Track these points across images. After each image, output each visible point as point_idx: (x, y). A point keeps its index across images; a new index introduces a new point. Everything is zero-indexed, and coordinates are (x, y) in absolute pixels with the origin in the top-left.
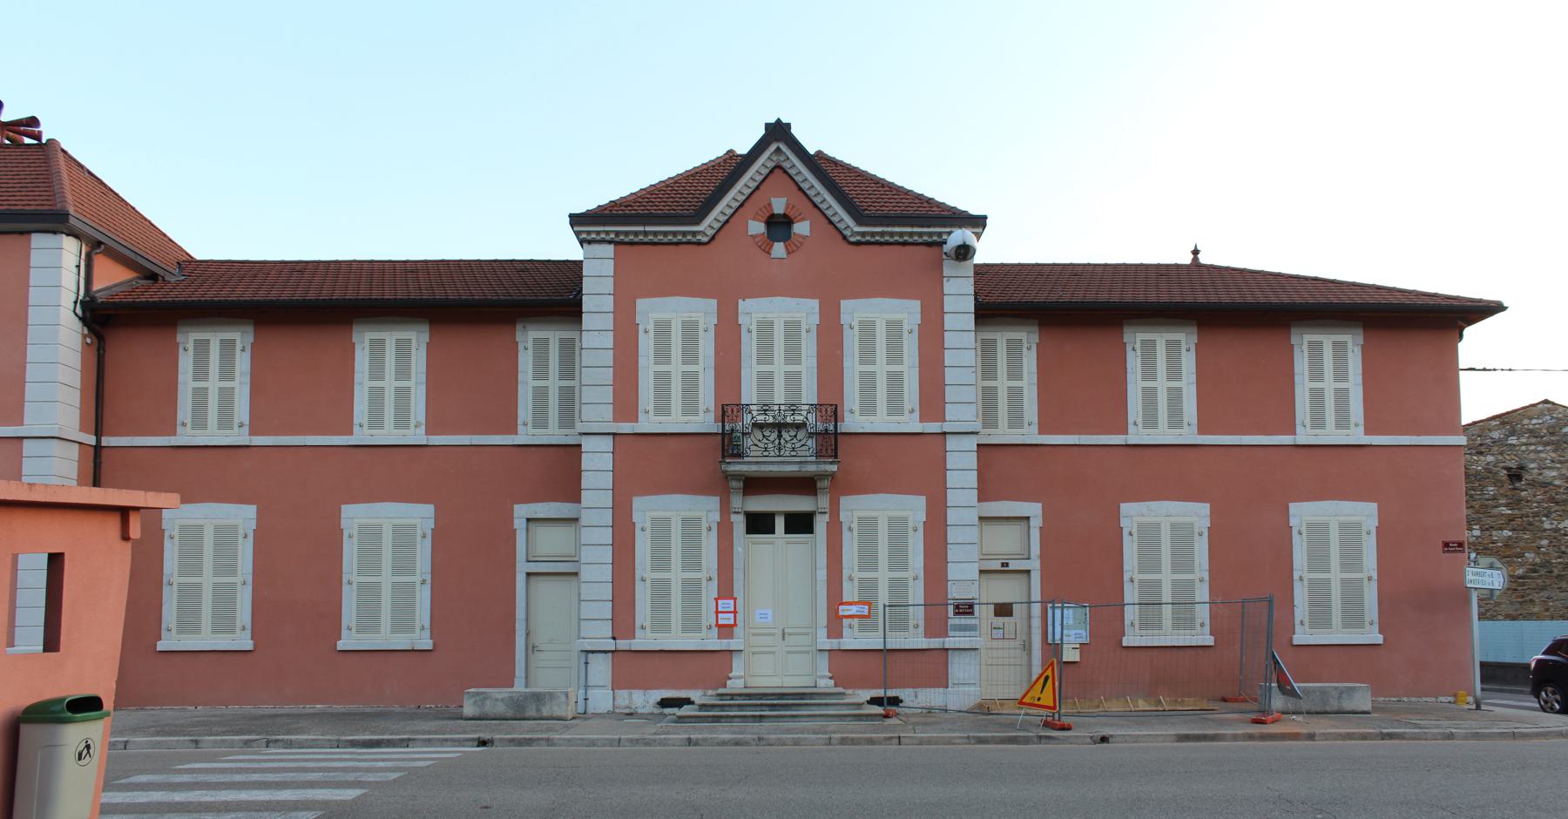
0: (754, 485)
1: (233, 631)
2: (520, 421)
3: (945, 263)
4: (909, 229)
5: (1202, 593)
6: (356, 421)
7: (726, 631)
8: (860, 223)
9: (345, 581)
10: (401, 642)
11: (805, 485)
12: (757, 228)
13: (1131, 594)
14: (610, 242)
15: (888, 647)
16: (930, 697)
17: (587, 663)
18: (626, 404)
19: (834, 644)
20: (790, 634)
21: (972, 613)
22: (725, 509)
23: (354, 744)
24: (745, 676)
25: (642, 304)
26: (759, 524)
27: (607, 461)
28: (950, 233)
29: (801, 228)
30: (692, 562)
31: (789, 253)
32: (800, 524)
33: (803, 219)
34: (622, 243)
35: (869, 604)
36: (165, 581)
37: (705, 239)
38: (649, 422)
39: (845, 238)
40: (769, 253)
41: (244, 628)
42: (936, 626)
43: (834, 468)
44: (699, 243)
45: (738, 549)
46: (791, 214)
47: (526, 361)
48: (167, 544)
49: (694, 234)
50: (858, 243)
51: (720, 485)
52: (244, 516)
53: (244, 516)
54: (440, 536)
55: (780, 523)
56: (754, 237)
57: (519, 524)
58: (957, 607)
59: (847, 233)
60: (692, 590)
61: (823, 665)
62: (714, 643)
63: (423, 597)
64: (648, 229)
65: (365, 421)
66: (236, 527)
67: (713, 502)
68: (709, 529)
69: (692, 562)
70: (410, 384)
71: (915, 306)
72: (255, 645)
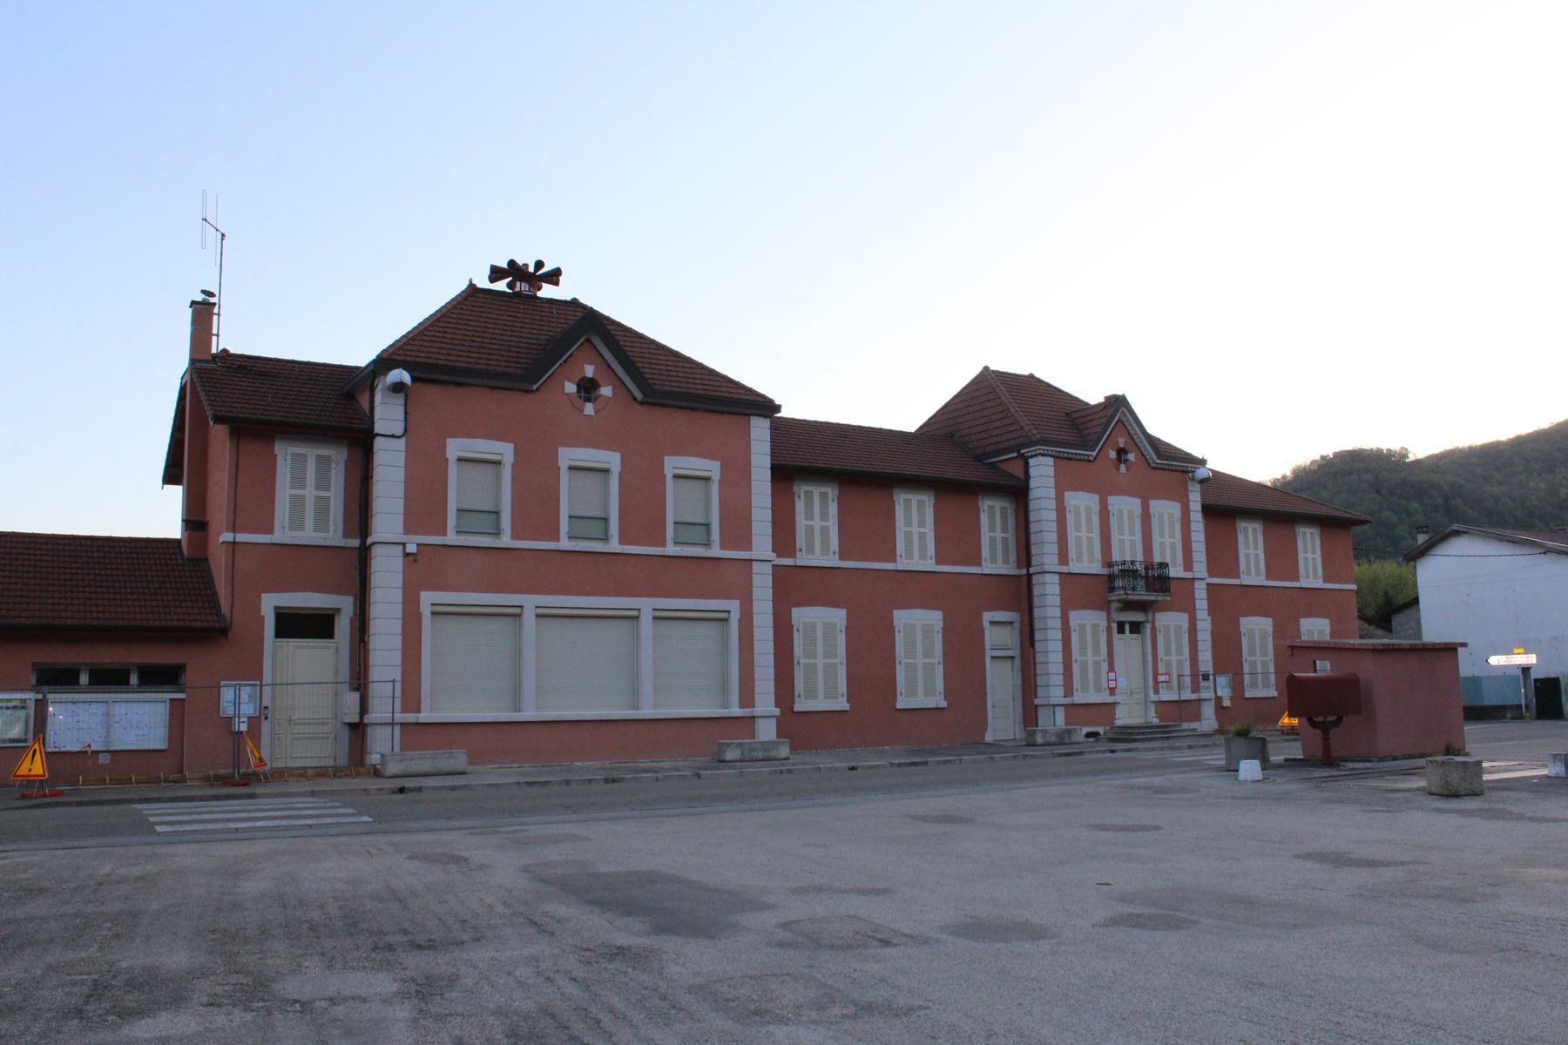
0: (1128, 606)
1: (836, 698)
2: (983, 558)
3: (1189, 483)
4: (1165, 462)
5: (1272, 669)
6: (898, 553)
7: (1112, 691)
8: (1159, 458)
9: (897, 662)
10: (929, 703)
11: (1143, 606)
12: (1113, 454)
13: (1246, 669)
14: (1052, 456)
15: (1182, 698)
16: (1194, 725)
17: (1054, 713)
18: (1063, 558)
19: (1067, 701)
20: (1135, 693)
21: (1208, 680)
22: (1109, 620)
23: (1060, 755)
24: (1123, 717)
25: (1068, 495)
26: (1121, 630)
27: (1056, 589)
28: (1199, 468)
29: (1131, 457)
30: (1096, 652)
31: (1127, 470)
32: (1136, 628)
33: (1131, 452)
34: (1060, 458)
35: (1169, 674)
36: (795, 661)
37: (1091, 458)
38: (1075, 567)
39: (1149, 464)
40: (1119, 470)
41: (843, 695)
42: (1195, 688)
43: (1169, 598)
44: (1089, 461)
45: (1116, 642)
46: (1127, 448)
47: (984, 520)
48: (795, 635)
49: (1088, 455)
50: (1154, 468)
51: (1105, 606)
52: (838, 616)
53: (838, 616)
54: (946, 631)
55: (1127, 628)
56: (1112, 460)
57: (986, 624)
58: (1203, 675)
59: (1151, 461)
60: (1097, 664)
61: (1152, 709)
62: (1110, 699)
63: (939, 671)
64: (1073, 451)
65: (903, 555)
66: (835, 624)
67: (1103, 615)
68: (1103, 631)
69: (1179, 652)
70: (830, 524)
71: (1178, 505)
72: (851, 707)
